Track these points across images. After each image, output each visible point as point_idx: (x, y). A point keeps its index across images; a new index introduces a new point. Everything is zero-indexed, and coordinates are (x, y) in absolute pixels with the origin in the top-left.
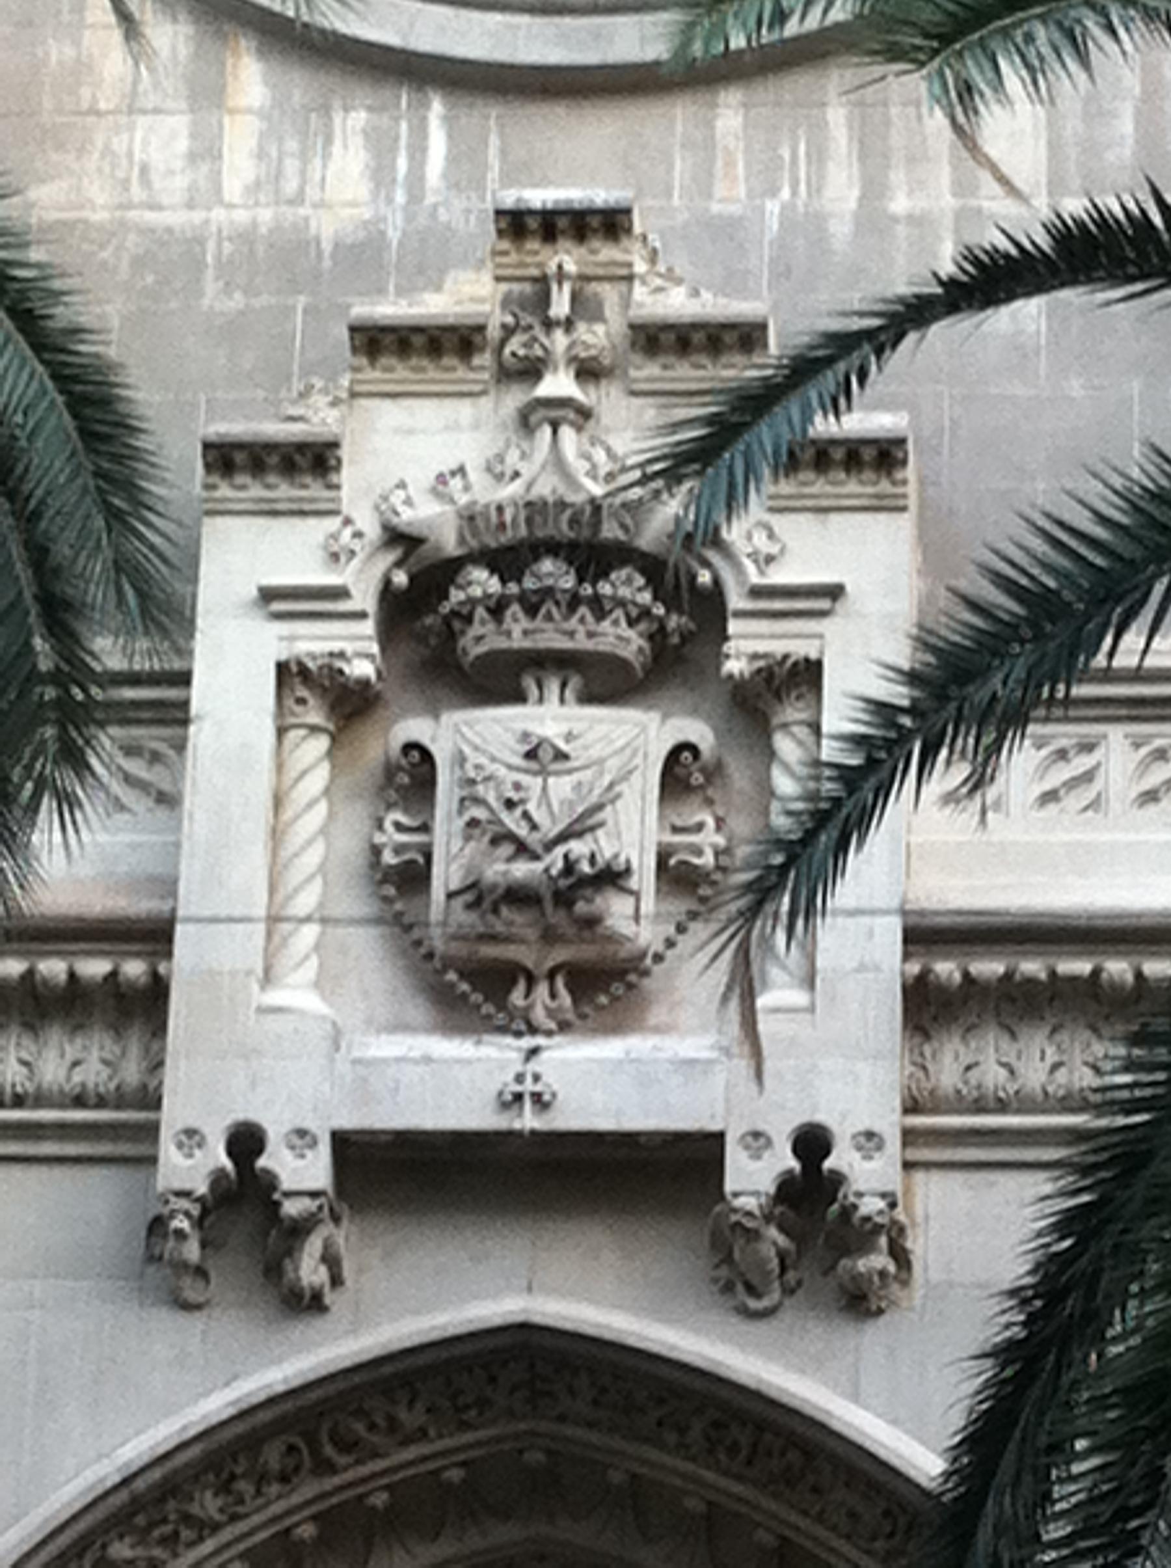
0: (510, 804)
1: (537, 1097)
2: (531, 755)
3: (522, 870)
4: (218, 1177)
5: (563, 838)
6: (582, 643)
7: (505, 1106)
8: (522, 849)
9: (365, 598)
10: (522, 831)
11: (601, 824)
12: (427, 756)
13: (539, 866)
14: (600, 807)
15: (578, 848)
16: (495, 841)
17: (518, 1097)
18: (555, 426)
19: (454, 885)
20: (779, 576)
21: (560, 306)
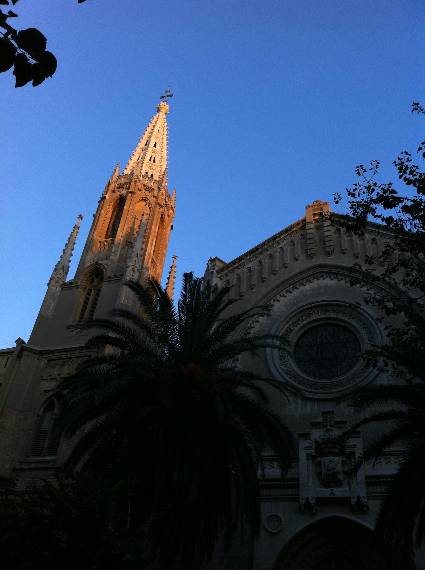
0: (328, 466)
1: (333, 494)
2: (330, 461)
3: (330, 472)
4: (305, 502)
5: (333, 469)
6: (333, 451)
7: (330, 495)
8: (330, 471)
9: (314, 447)
10: (329, 469)
11: (336, 468)
12: (321, 462)
13: (331, 472)
14: (336, 466)
15: (335, 470)
16: (327, 470)
17: (331, 494)
18: (329, 431)
19: (324, 474)
20: (350, 444)
21: (328, 420)
